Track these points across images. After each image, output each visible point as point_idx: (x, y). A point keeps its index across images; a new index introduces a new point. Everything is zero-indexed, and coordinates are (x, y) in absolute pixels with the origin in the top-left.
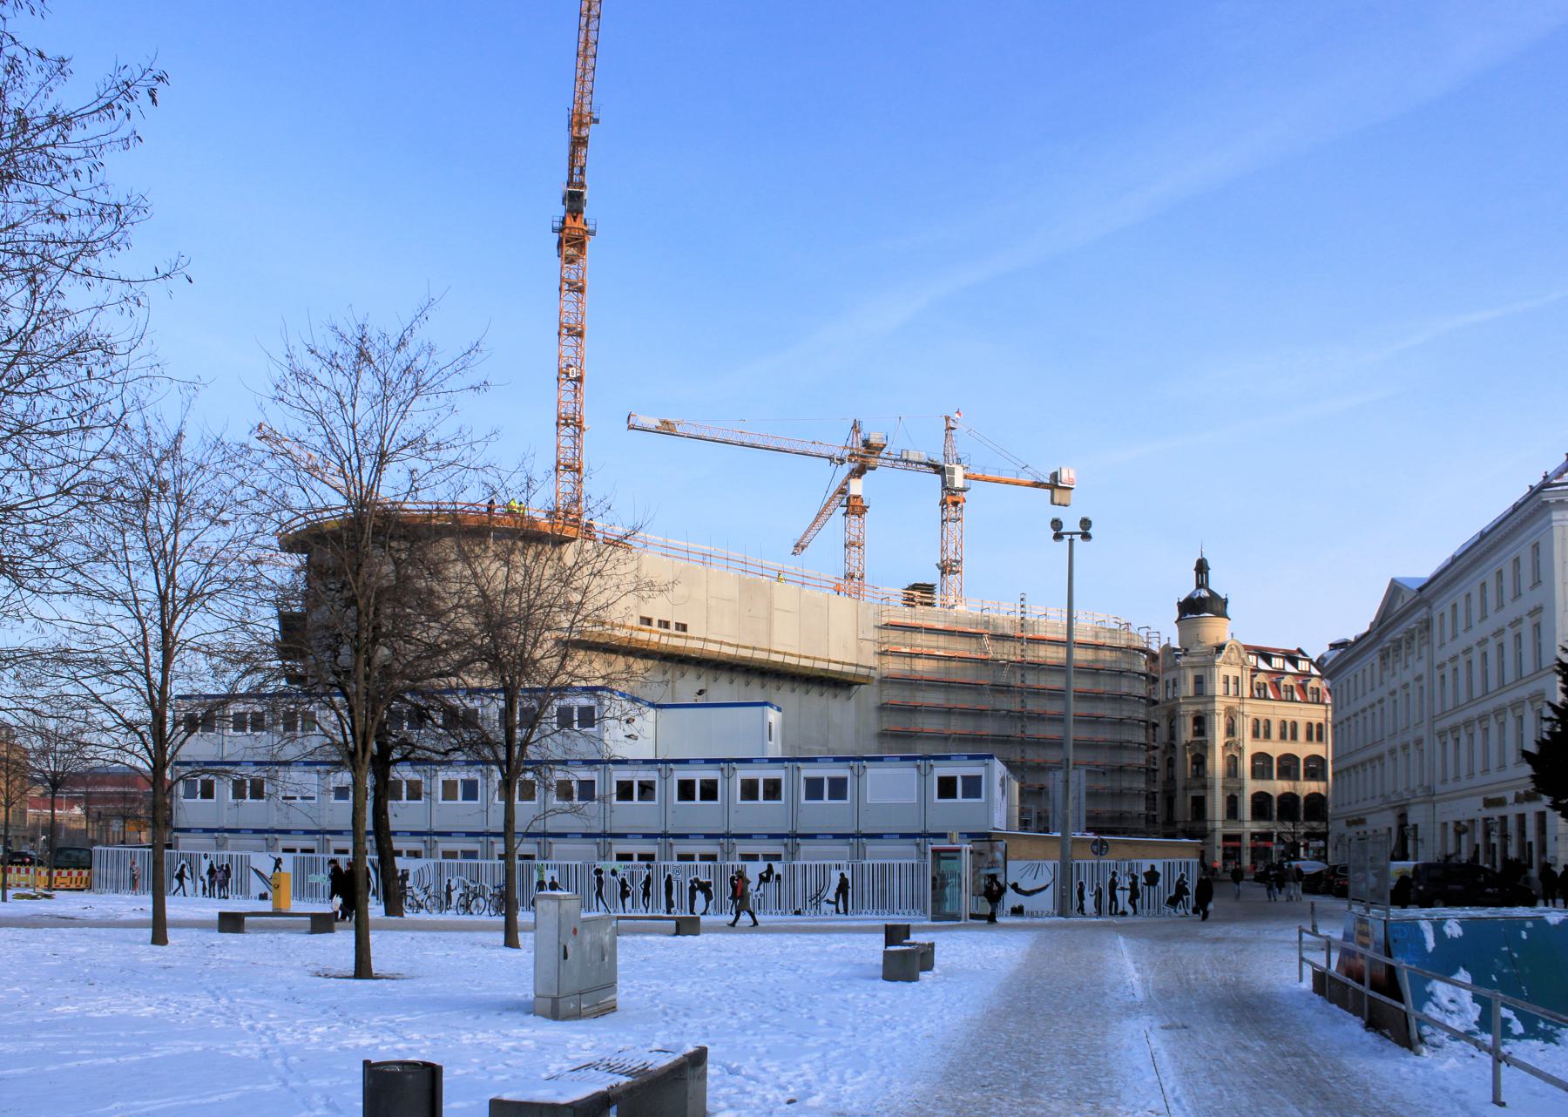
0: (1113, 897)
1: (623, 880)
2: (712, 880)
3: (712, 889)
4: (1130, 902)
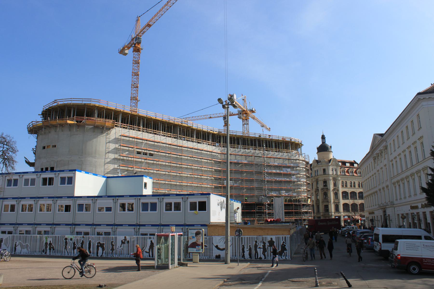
0: (256, 252)
1: (74, 242)
2: (105, 243)
3: (104, 246)
4: (263, 254)
